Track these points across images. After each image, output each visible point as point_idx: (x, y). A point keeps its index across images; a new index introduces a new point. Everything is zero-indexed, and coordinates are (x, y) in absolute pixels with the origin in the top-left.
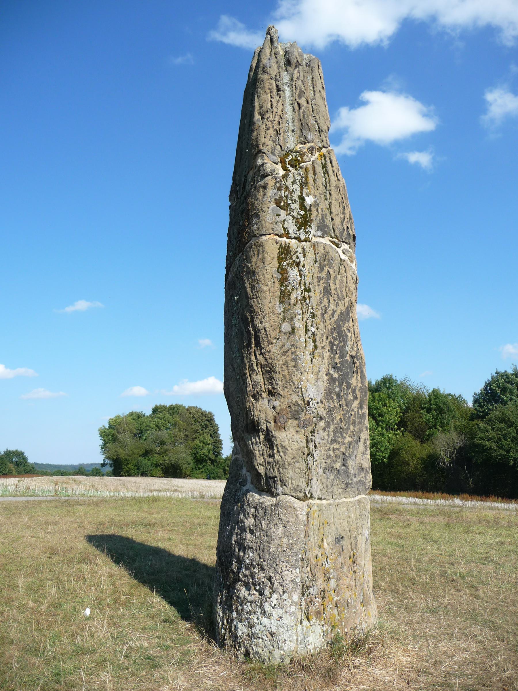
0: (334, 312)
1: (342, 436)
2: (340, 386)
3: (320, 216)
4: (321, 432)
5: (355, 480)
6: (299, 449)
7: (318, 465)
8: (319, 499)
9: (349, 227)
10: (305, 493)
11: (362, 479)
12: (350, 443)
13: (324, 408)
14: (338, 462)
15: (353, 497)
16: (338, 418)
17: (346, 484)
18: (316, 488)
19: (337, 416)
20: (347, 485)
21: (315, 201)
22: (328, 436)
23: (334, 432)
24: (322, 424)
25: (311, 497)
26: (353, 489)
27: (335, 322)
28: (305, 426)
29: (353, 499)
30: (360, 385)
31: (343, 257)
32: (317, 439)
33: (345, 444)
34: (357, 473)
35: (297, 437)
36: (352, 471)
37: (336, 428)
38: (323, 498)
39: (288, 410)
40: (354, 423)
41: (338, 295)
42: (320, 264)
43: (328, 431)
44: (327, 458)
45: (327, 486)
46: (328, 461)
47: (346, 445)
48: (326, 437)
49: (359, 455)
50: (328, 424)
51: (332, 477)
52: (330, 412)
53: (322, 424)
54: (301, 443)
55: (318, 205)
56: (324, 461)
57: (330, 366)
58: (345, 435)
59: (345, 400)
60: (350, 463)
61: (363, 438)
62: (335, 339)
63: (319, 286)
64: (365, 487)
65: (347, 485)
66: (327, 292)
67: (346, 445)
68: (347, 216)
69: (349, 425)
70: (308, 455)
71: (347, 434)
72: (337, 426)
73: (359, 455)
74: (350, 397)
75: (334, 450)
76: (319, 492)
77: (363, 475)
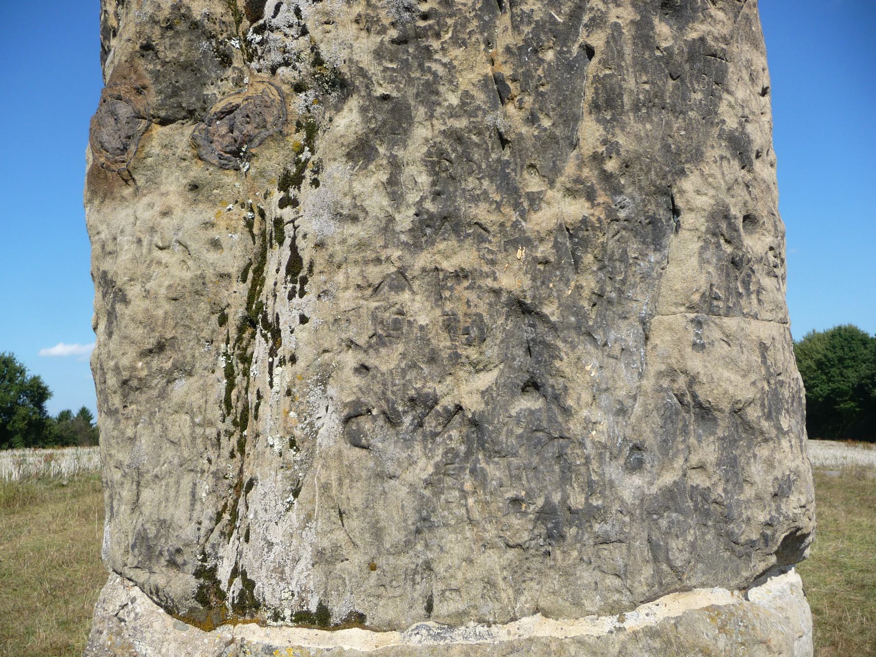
1: (511, 191)
4: (337, 171)
5: (631, 486)
6: (198, 288)
7: (306, 384)
8: (302, 618)
10: (207, 574)
11: (698, 480)
12: (575, 235)
14: (478, 368)
15: (617, 610)
16: (468, 80)
17: (546, 513)
18: (278, 545)
19: (468, 69)
20: (554, 524)
22: (396, 198)
23: (436, 161)
24: (347, 121)
25: (248, 605)
26: (616, 555)
28: (237, 154)
29: (608, 623)
32: (311, 219)
33: (527, 242)
34: (651, 440)
35: (189, 219)
36: (593, 421)
37: (457, 137)
38: (339, 610)
39: (145, 66)
40: (608, 103)
43: (396, 165)
44: (379, 341)
45: (377, 533)
46: (387, 361)
48: (377, 202)
49: (672, 326)
50: (392, 119)
51: (424, 468)
53: (347, 121)
54: (212, 256)
56: (350, 359)
58: (533, 183)
60: (581, 369)
61: (704, 202)
64: (731, 540)
65: (554, 524)
67: (544, 250)
69: (571, 120)
70: (249, 322)
71: (550, 177)
72: (461, 123)
73: (672, 326)
75: (440, 283)
76: (304, 576)
77: (708, 451)
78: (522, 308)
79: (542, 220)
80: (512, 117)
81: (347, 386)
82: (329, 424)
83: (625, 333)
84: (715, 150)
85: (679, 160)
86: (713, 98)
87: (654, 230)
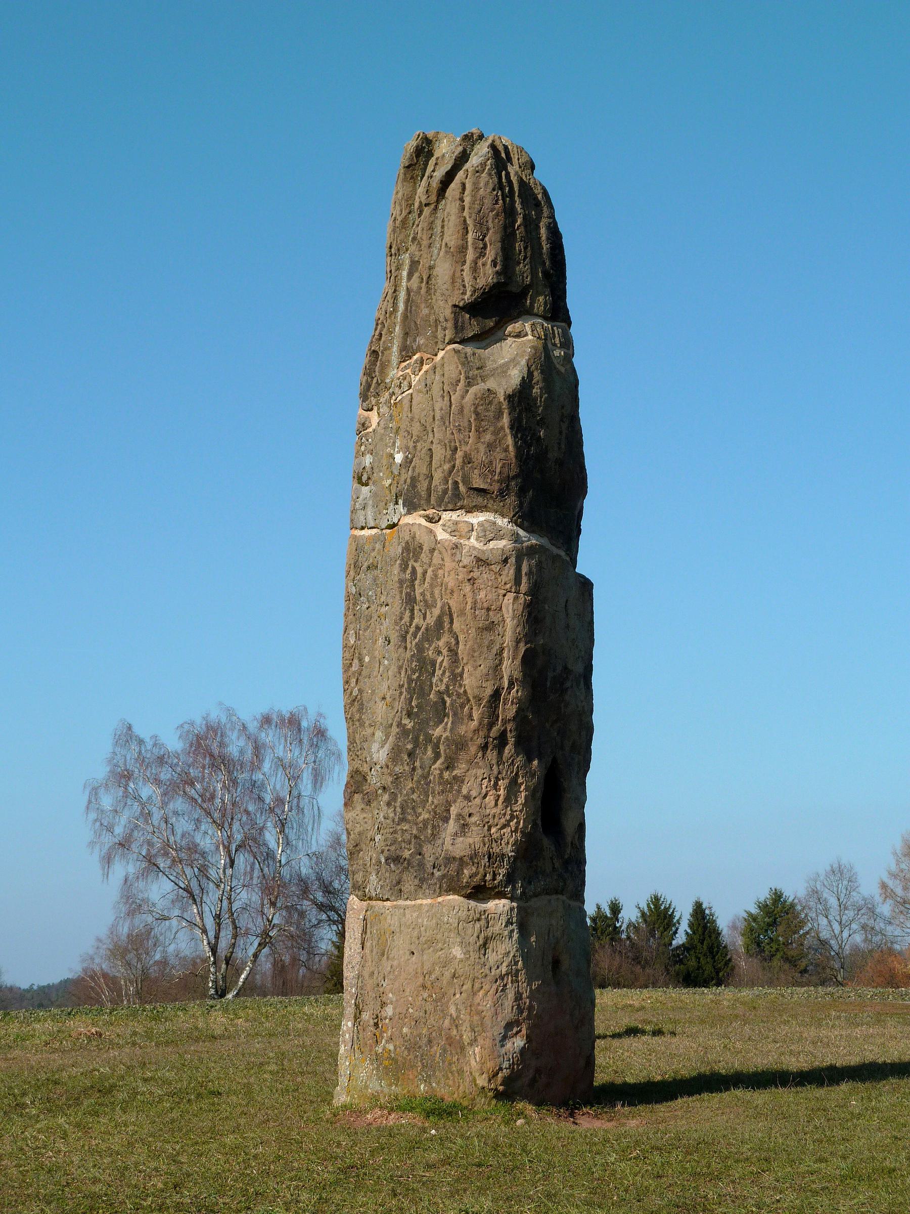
0: (418, 628)
1: (415, 812)
2: (416, 741)
3: (409, 481)
9: (459, 479)
12: (425, 823)
13: (390, 775)
20: (422, 880)
21: (407, 457)
22: (395, 814)
23: (402, 808)
27: (416, 644)
30: (448, 734)
31: (442, 535)
36: (429, 860)
41: (426, 601)
42: (403, 560)
43: (395, 807)
46: (393, 848)
47: (421, 825)
48: (392, 815)
49: (448, 840)
50: (394, 797)
52: (397, 779)
55: (411, 462)
56: (387, 848)
57: (404, 713)
59: (421, 759)
60: (427, 849)
62: (414, 672)
63: (401, 592)
65: (422, 880)
66: (410, 600)
68: (458, 462)
74: (430, 753)
78: (416, 837)
79: (421, 818)
80: (415, 796)
81: (386, 853)
82: (383, 860)
83: (440, 842)
84: (460, 799)
85: (448, 804)
86: (460, 787)
87: (446, 820)
